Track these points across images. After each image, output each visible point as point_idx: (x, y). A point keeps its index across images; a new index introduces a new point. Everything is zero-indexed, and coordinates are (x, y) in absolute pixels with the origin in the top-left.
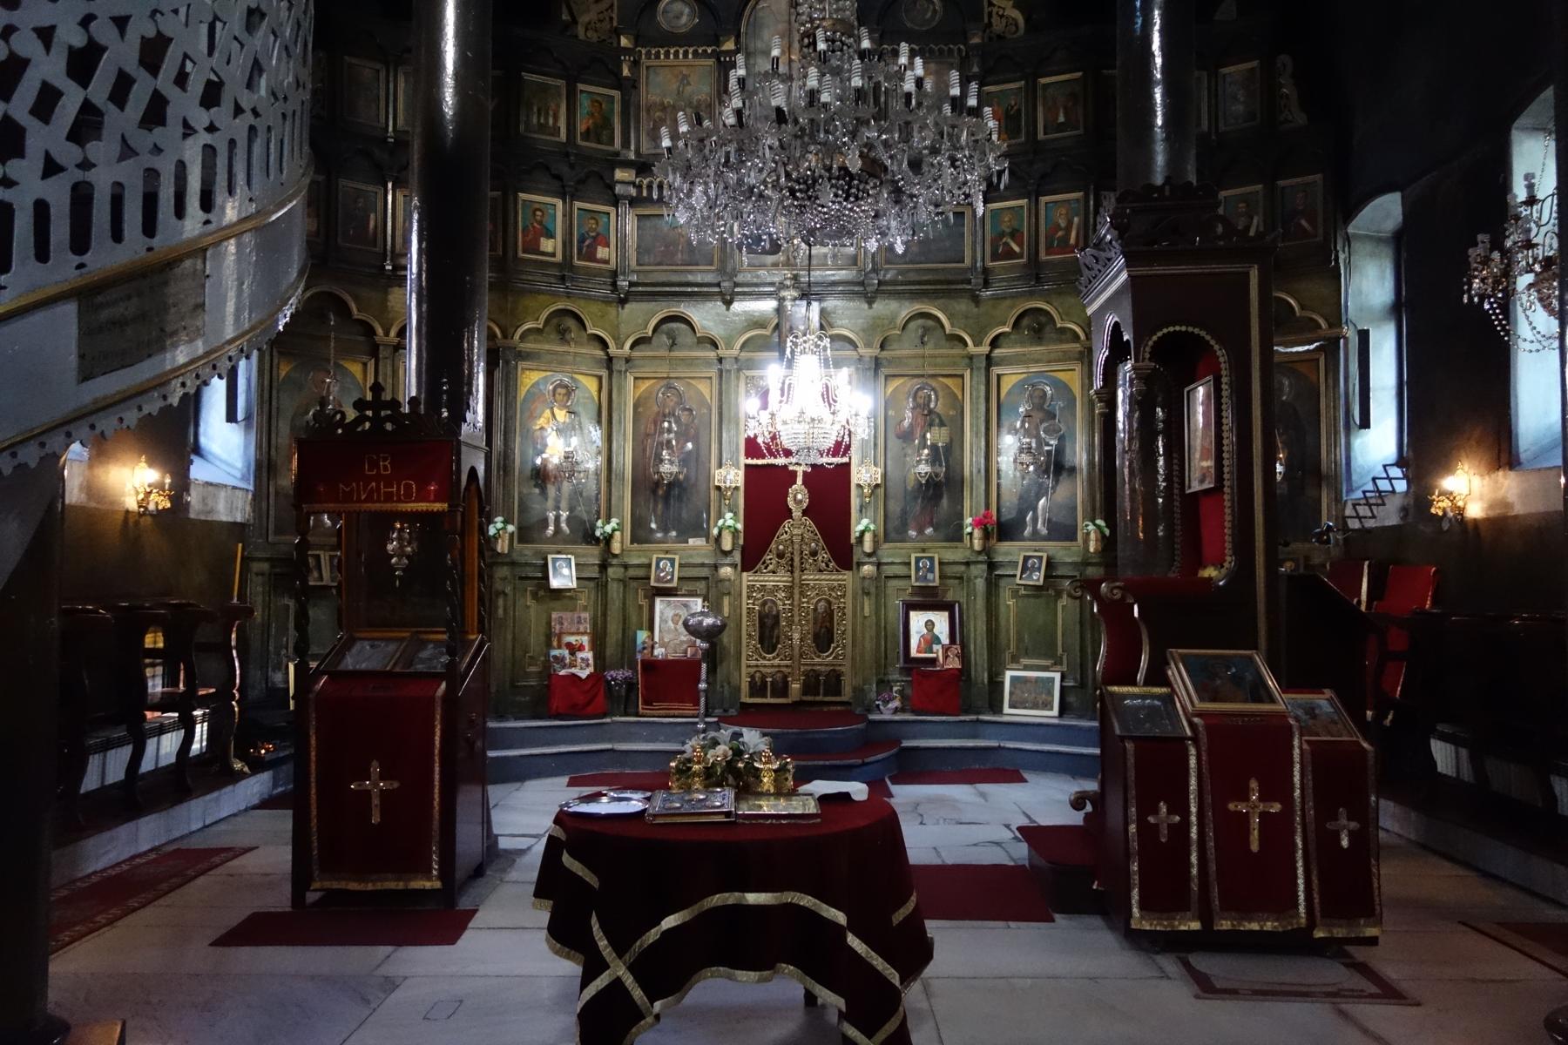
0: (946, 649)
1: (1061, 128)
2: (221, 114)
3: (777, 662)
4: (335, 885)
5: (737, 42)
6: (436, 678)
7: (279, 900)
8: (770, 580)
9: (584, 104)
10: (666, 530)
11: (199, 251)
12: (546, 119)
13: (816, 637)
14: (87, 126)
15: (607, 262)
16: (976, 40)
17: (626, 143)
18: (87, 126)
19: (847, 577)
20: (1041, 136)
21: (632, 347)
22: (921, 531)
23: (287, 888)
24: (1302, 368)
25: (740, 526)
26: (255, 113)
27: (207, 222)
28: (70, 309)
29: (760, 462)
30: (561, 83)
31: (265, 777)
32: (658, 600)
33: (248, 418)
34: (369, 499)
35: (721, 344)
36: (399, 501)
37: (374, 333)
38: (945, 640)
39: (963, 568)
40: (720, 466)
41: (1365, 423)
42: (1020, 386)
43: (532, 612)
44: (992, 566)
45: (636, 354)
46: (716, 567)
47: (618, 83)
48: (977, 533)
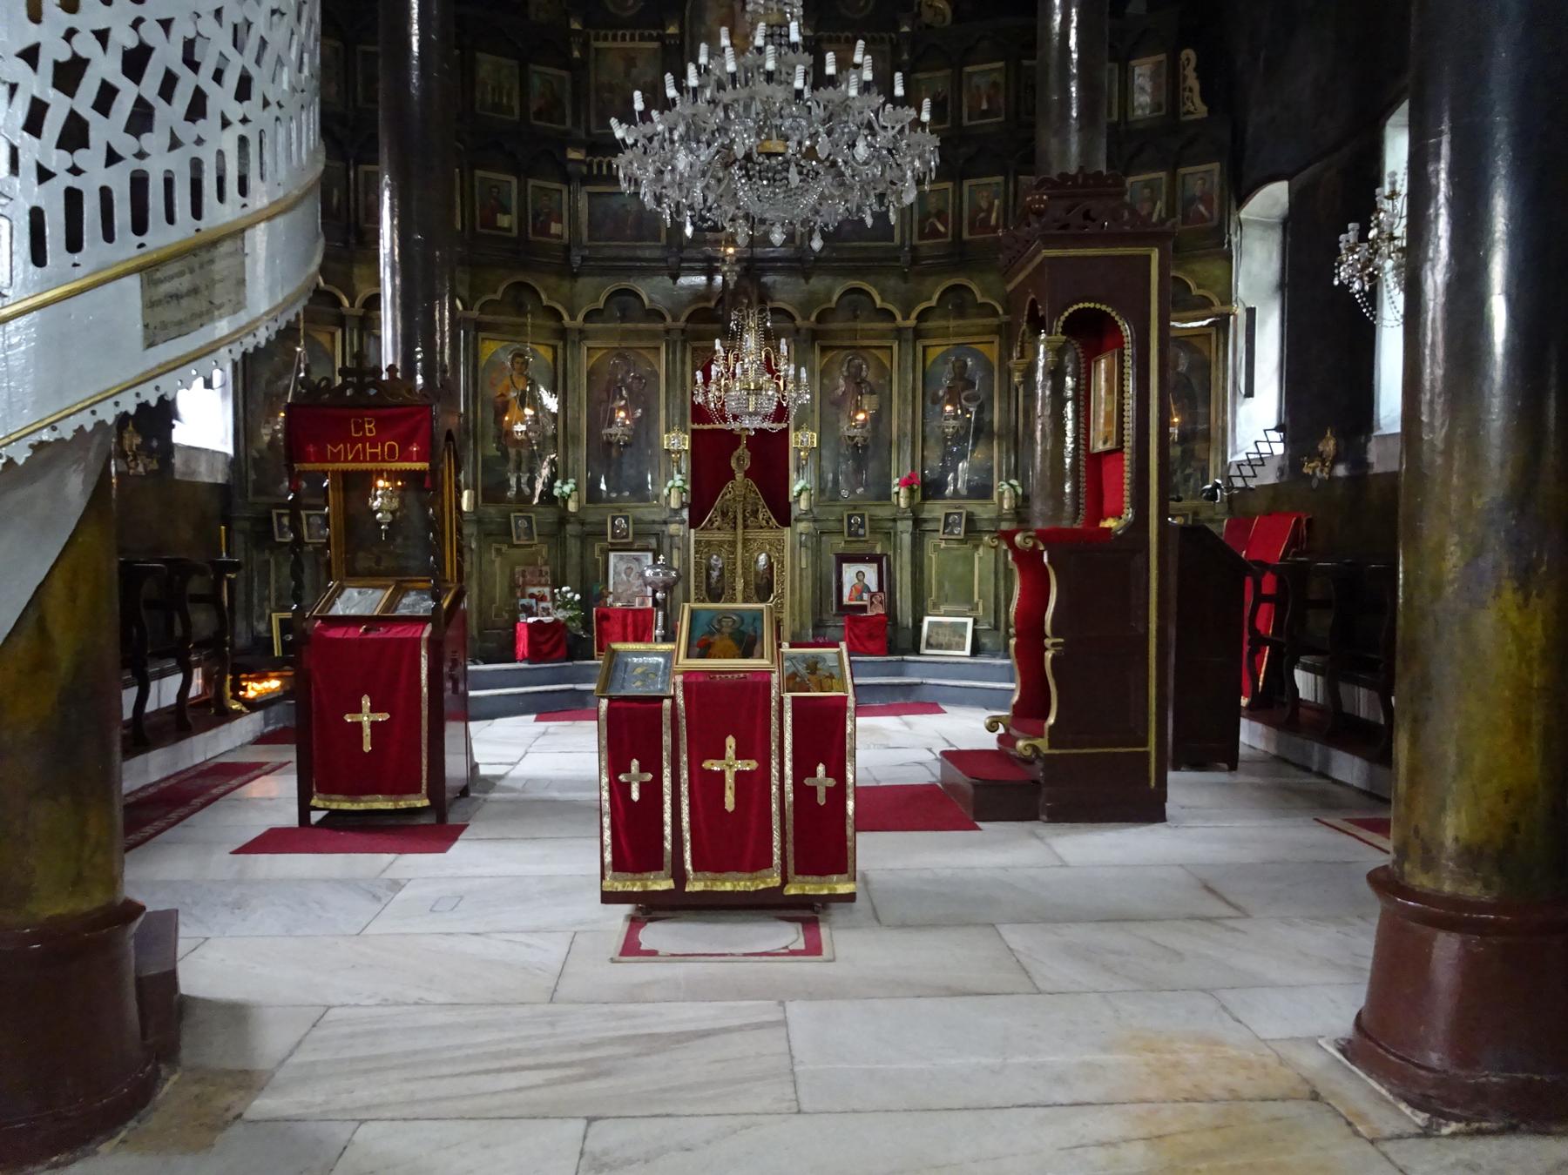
0: (873, 595)
1: (985, 114)
2: (252, 107)
4: (334, 806)
5: (681, 27)
6: (421, 621)
7: (288, 817)
8: (717, 536)
9: (536, 81)
10: (620, 492)
11: (237, 233)
12: (501, 99)
13: (758, 589)
14: (141, 119)
15: (560, 237)
16: (906, 29)
17: (576, 122)
18: (141, 119)
19: (787, 531)
20: (966, 122)
21: (587, 318)
22: (853, 491)
23: (295, 810)
24: (1195, 341)
25: (688, 487)
26: (280, 106)
27: (244, 205)
28: (134, 282)
29: (706, 427)
30: (514, 63)
31: (258, 715)
32: (612, 555)
33: (223, 385)
34: (356, 459)
35: (669, 319)
36: (383, 460)
37: (339, 303)
38: (874, 588)
39: (890, 524)
40: (668, 431)
41: (1250, 393)
42: (944, 358)
43: (497, 564)
44: (918, 522)
45: (589, 326)
46: (665, 523)
47: (568, 64)
48: (903, 492)
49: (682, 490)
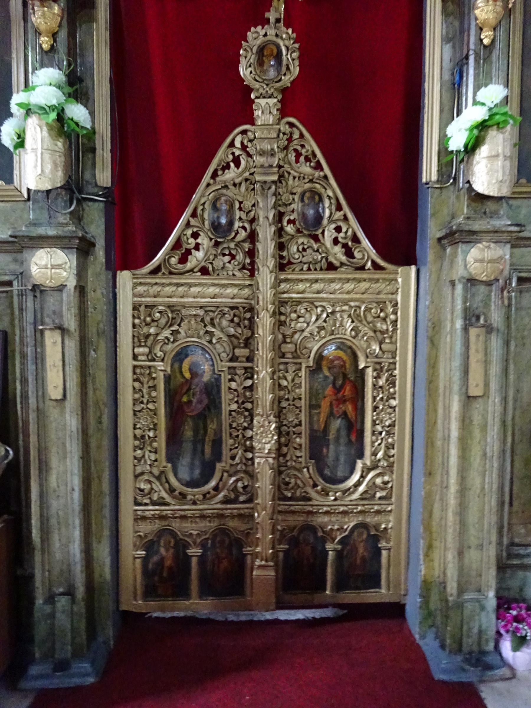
3: (215, 504)
49: (75, 144)
